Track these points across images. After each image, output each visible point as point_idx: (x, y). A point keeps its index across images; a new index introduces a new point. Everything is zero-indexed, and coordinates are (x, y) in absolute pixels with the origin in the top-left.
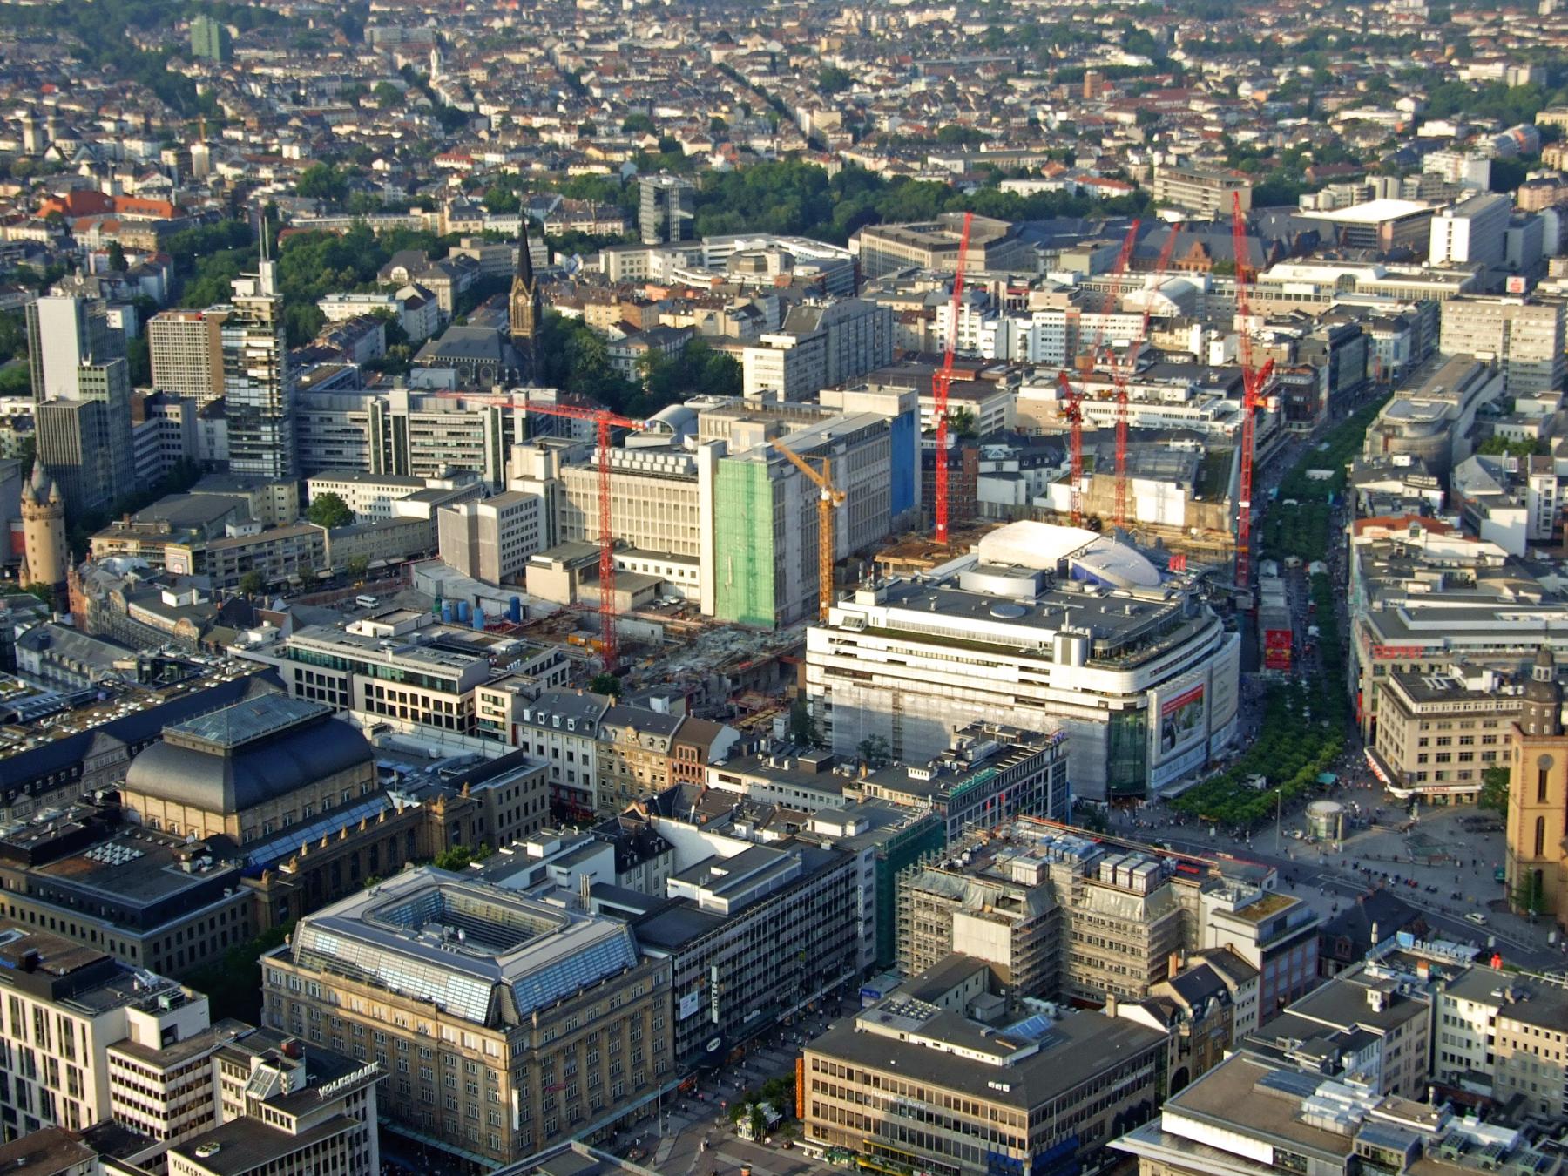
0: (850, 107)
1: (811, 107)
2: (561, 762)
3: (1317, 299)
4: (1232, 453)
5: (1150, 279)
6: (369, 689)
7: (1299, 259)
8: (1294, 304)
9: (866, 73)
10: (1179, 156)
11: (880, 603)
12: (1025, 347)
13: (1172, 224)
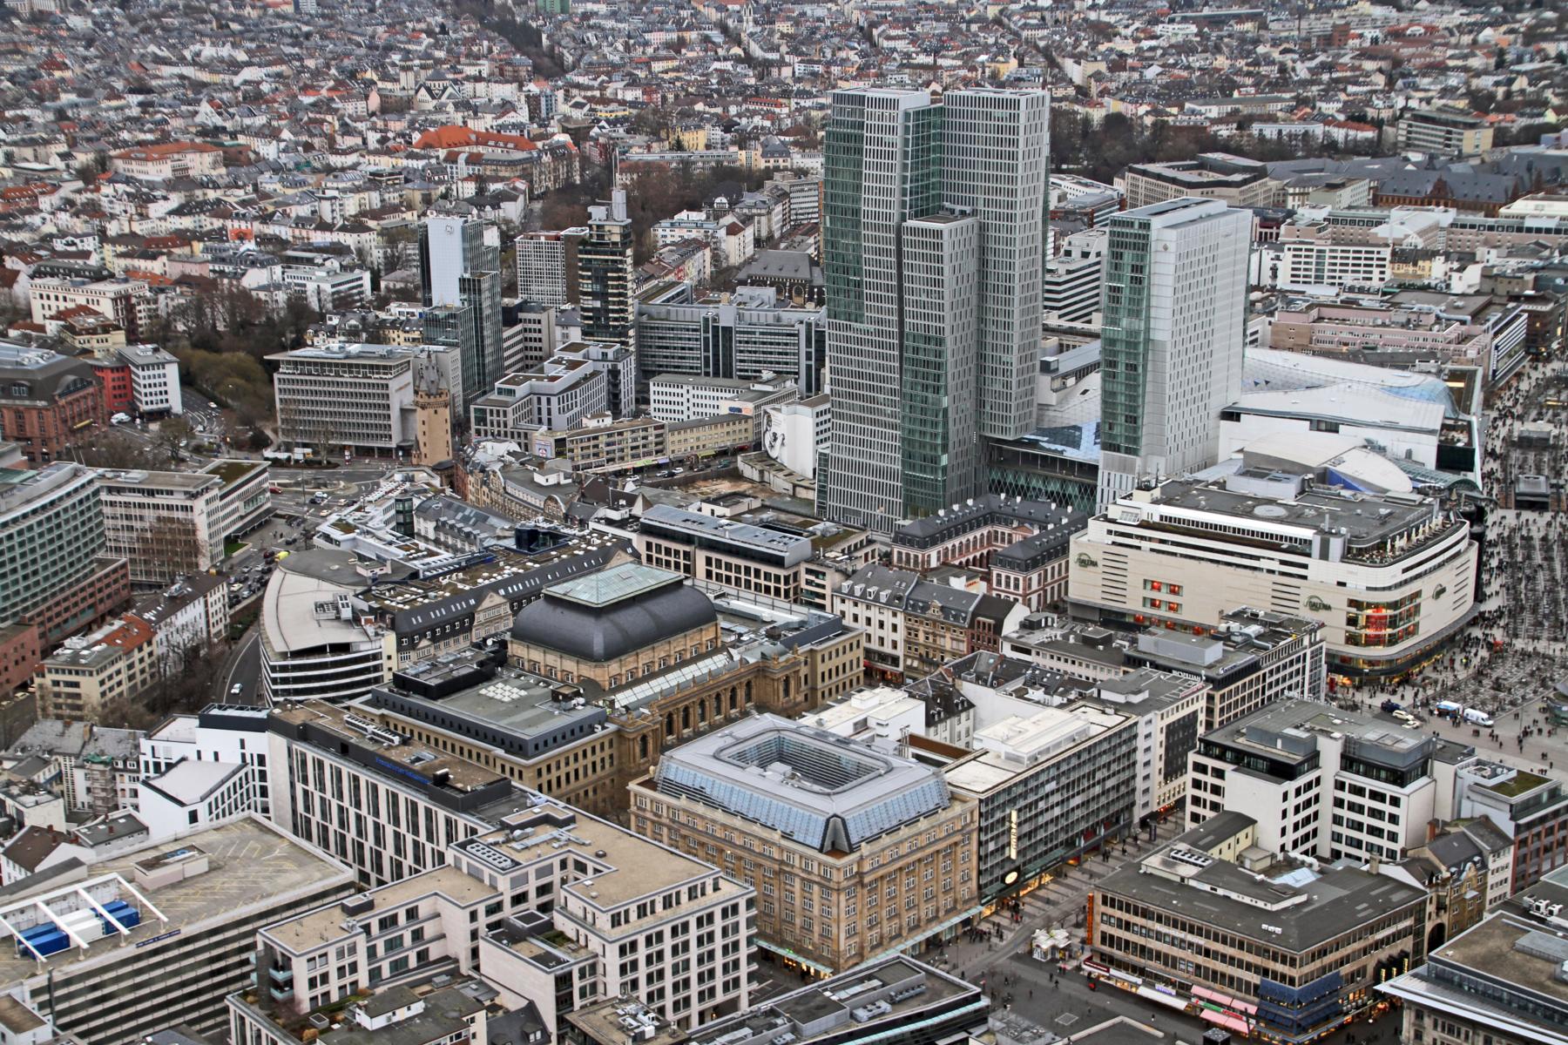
0: (1114, 56)
1: (1078, 58)
2: (874, 630)
3: (1558, 231)
4: (1475, 372)
5: (1396, 213)
6: (709, 561)
7: (1541, 194)
8: (1533, 237)
9: (1127, 27)
10: (1421, 100)
11: (1155, 502)
12: (1275, 276)
13: (1415, 164)
